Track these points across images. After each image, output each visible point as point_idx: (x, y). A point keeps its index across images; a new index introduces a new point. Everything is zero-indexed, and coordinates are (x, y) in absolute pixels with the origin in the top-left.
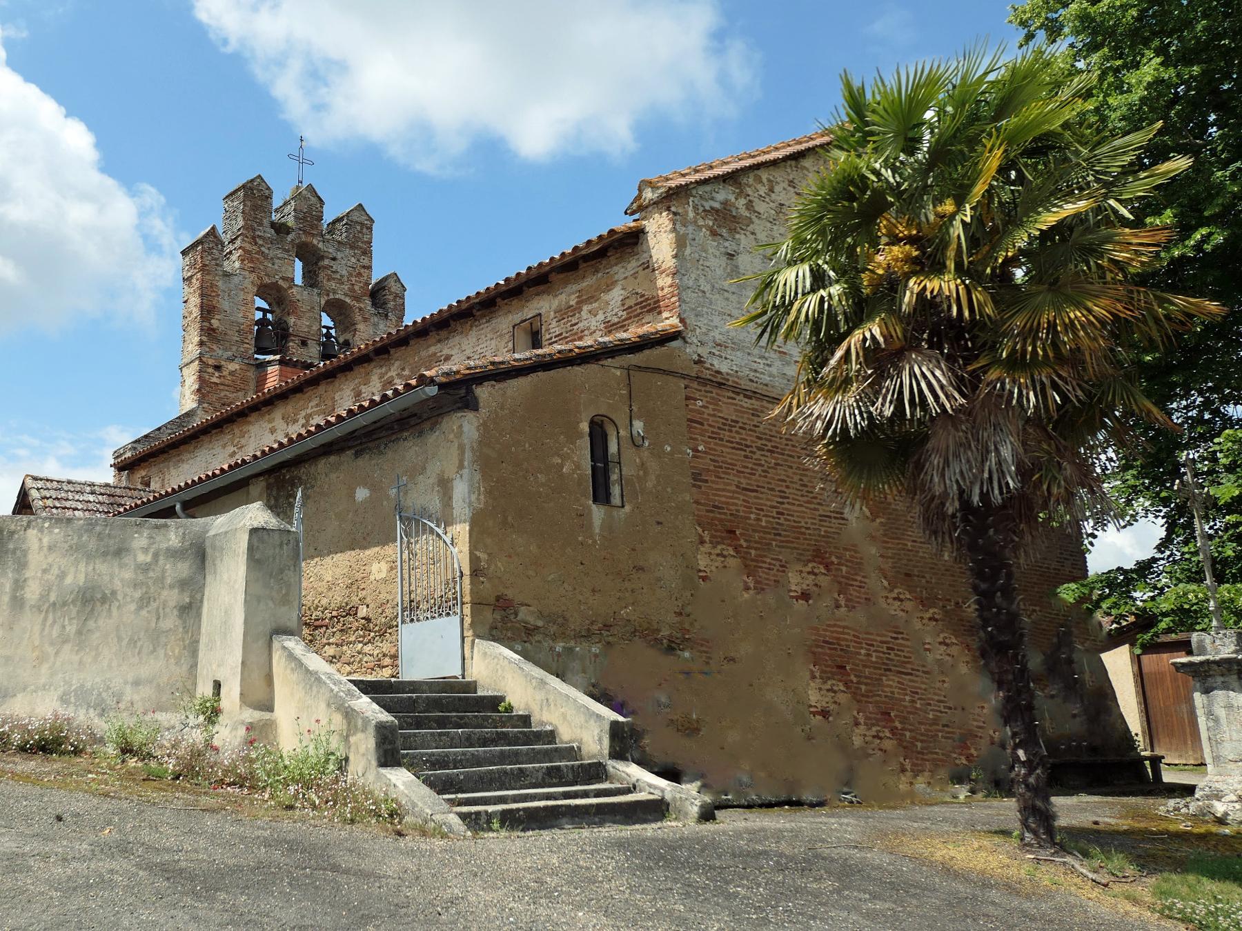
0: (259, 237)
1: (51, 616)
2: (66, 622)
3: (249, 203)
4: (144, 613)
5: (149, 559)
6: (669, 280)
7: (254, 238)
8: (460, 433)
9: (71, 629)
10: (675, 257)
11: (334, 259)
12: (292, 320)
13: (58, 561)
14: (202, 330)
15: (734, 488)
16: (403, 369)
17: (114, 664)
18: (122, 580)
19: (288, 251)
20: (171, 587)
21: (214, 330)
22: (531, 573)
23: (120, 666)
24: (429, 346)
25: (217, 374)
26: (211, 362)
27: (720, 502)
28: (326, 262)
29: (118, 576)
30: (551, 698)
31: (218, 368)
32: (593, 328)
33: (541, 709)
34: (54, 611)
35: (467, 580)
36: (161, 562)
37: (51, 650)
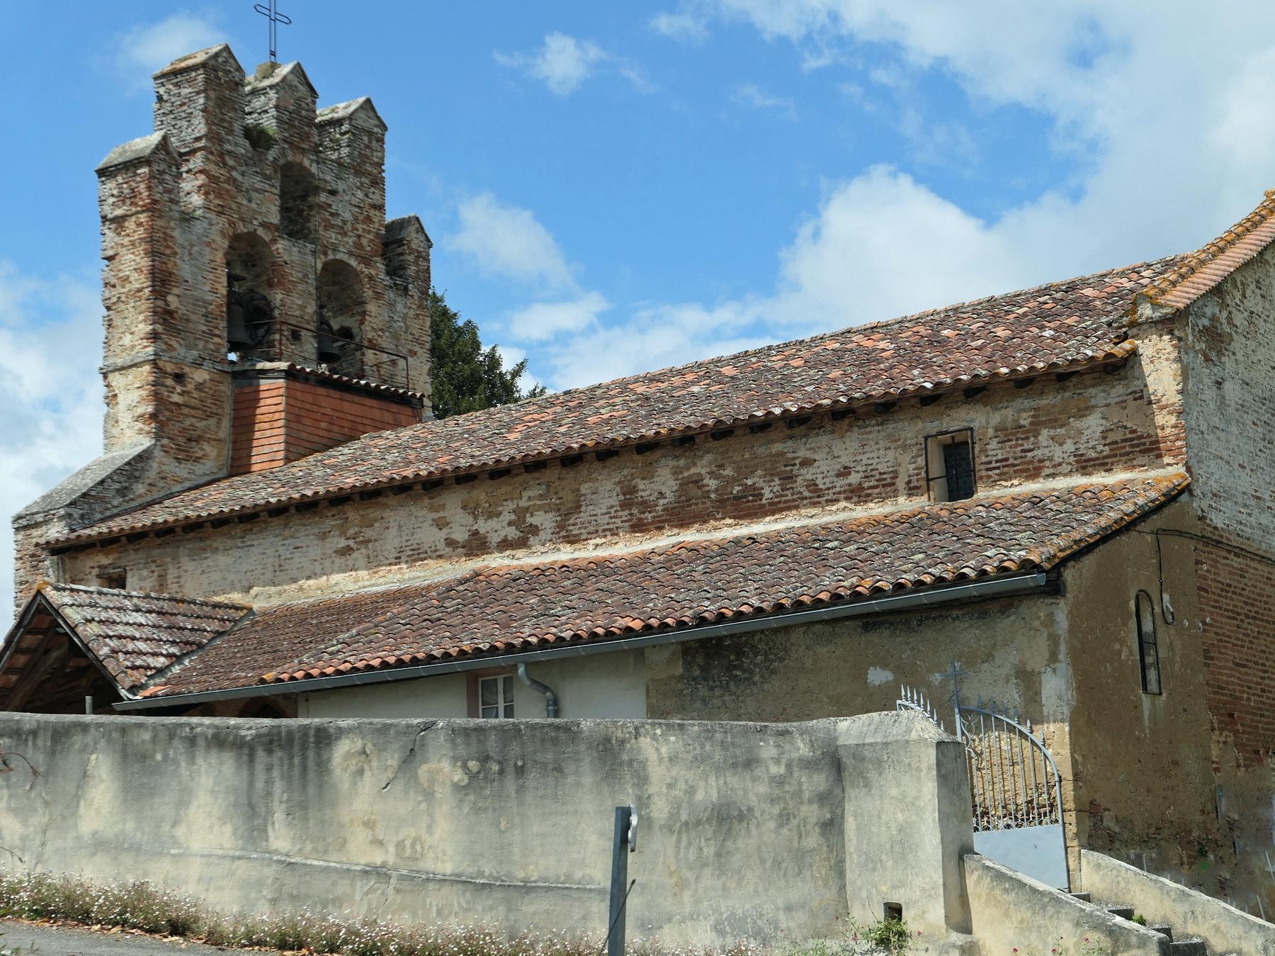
0: (229, 152)
1: (684, 837)
2: (703, 844)
3: (212, 94)
4: (785, 831)
5: (782, 770)
6: (1173, 420)
7: (221, 155)
8: (1051, 620)
9: (709, 851)
10: (1181, 392)
11: (333, 193)
12: (277, 296)
13: (685, 775)
14: (155, 313)
15: (1230, 664)
16: (721, 466)
17: (761, 888)
18: (757, 795)
19: (268, 178)
20: (810, 801)
21: (170, 313)
22: (1109, 774)
23: (766, 890)
24: (773, 441)
25: (179, 389)
26: (170, 368)
27: (1223, 682)
28: (323, 197)
29: (752, 791)
30: (1198, 910)
31: (179, 378)
32: (1057, 460)
33: (1185, 922)
34: (687, 831)
35: (1069, 787)
36: (796, 774)
37: (689, 875)
